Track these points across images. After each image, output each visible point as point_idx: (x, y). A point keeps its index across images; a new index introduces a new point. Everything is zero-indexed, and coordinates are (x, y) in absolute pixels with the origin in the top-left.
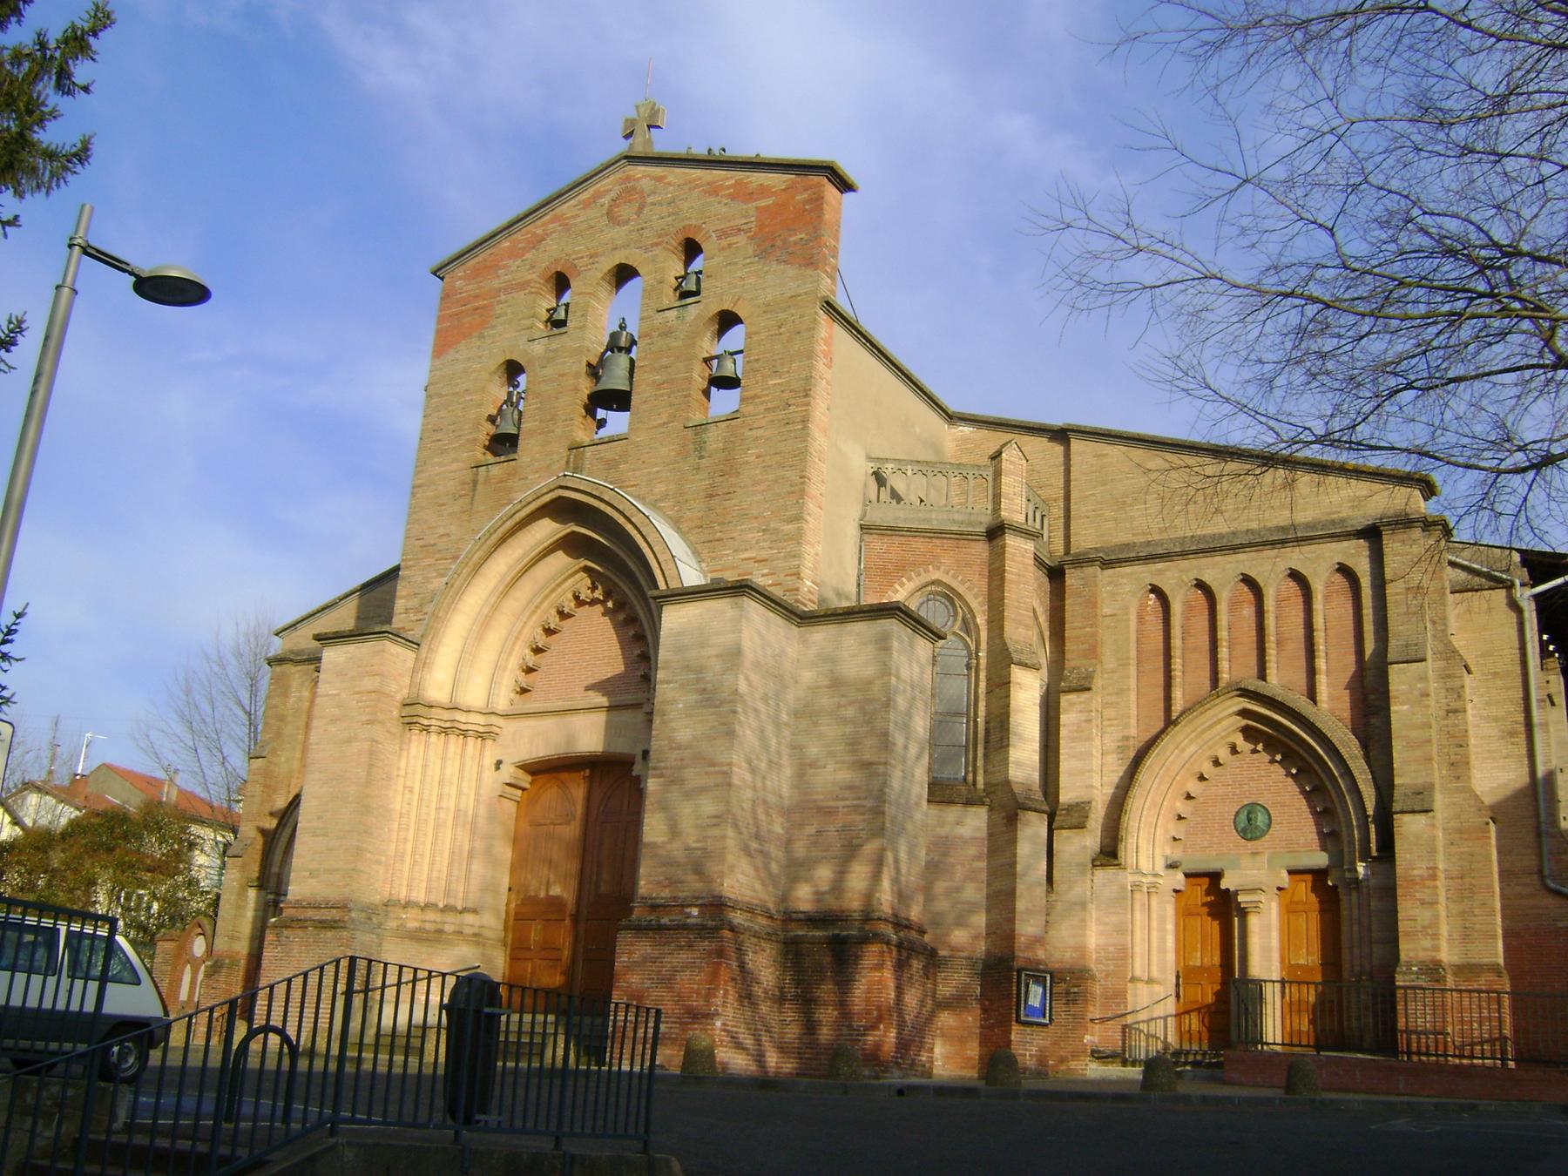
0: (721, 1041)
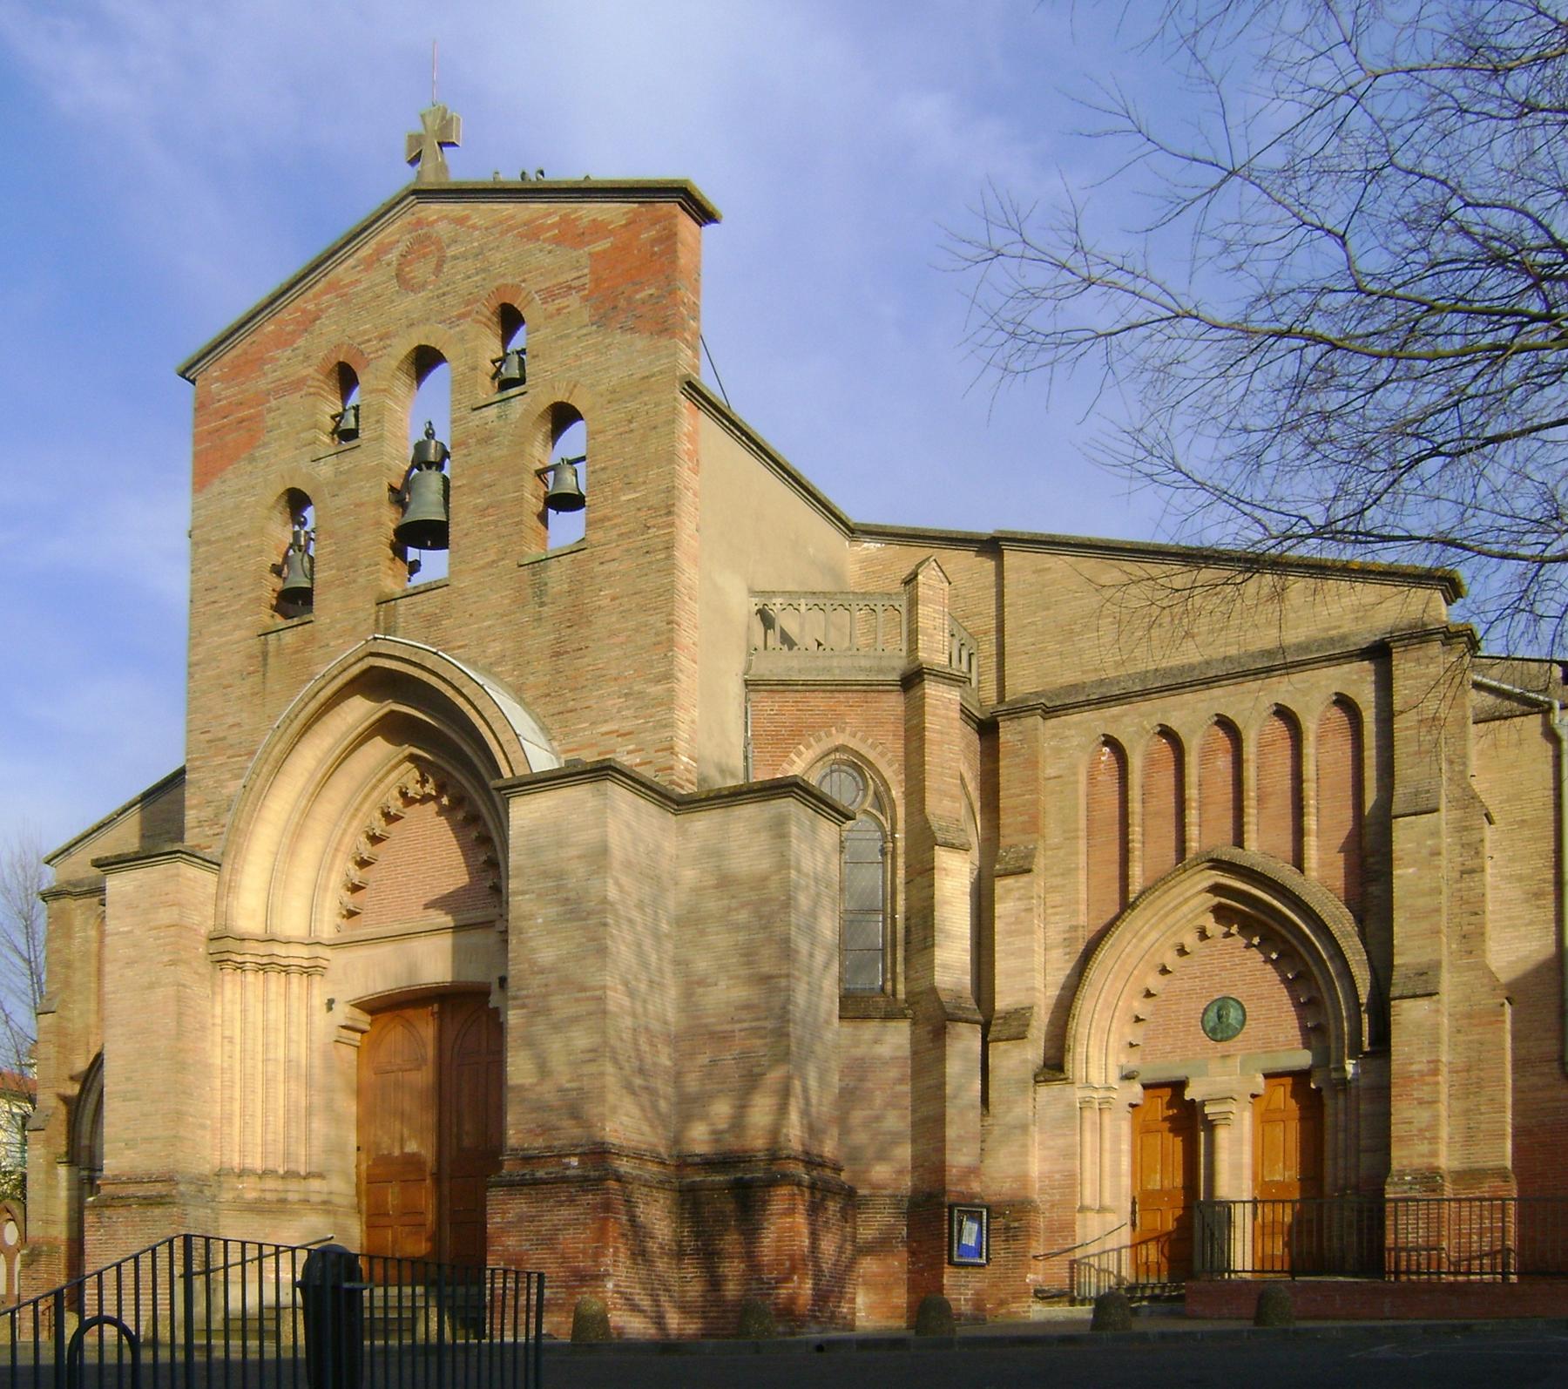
0: (614, 1304)
